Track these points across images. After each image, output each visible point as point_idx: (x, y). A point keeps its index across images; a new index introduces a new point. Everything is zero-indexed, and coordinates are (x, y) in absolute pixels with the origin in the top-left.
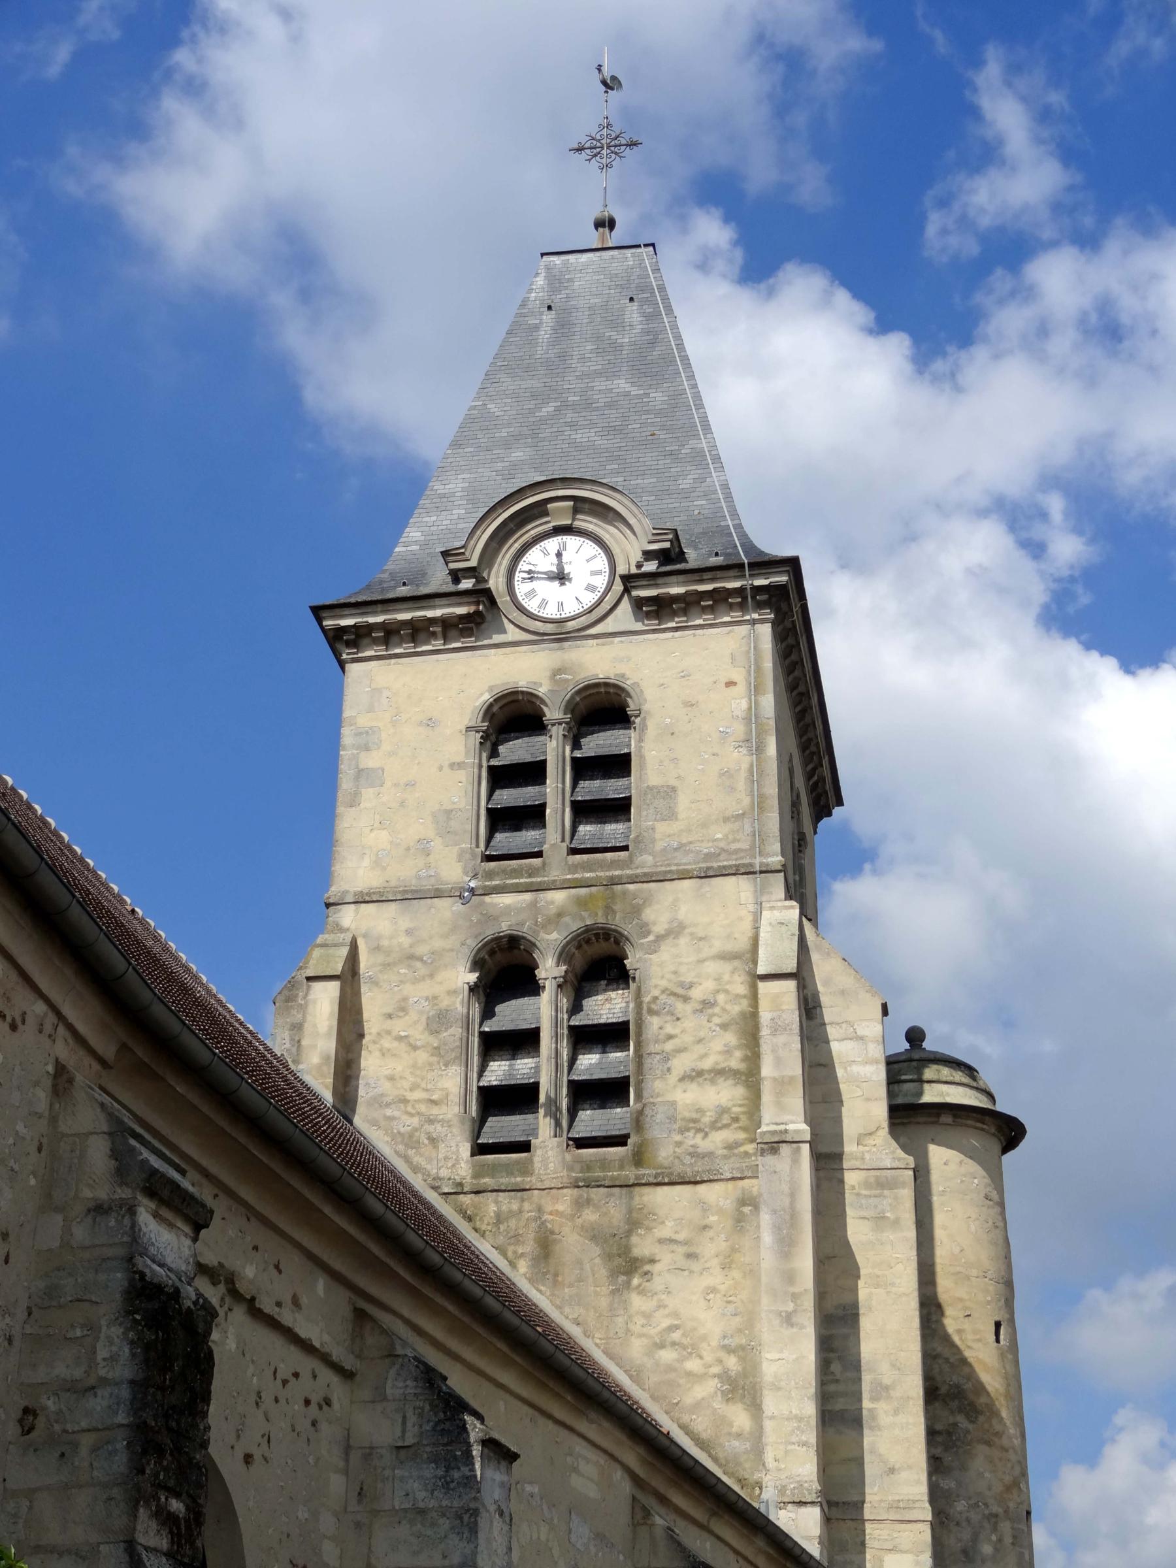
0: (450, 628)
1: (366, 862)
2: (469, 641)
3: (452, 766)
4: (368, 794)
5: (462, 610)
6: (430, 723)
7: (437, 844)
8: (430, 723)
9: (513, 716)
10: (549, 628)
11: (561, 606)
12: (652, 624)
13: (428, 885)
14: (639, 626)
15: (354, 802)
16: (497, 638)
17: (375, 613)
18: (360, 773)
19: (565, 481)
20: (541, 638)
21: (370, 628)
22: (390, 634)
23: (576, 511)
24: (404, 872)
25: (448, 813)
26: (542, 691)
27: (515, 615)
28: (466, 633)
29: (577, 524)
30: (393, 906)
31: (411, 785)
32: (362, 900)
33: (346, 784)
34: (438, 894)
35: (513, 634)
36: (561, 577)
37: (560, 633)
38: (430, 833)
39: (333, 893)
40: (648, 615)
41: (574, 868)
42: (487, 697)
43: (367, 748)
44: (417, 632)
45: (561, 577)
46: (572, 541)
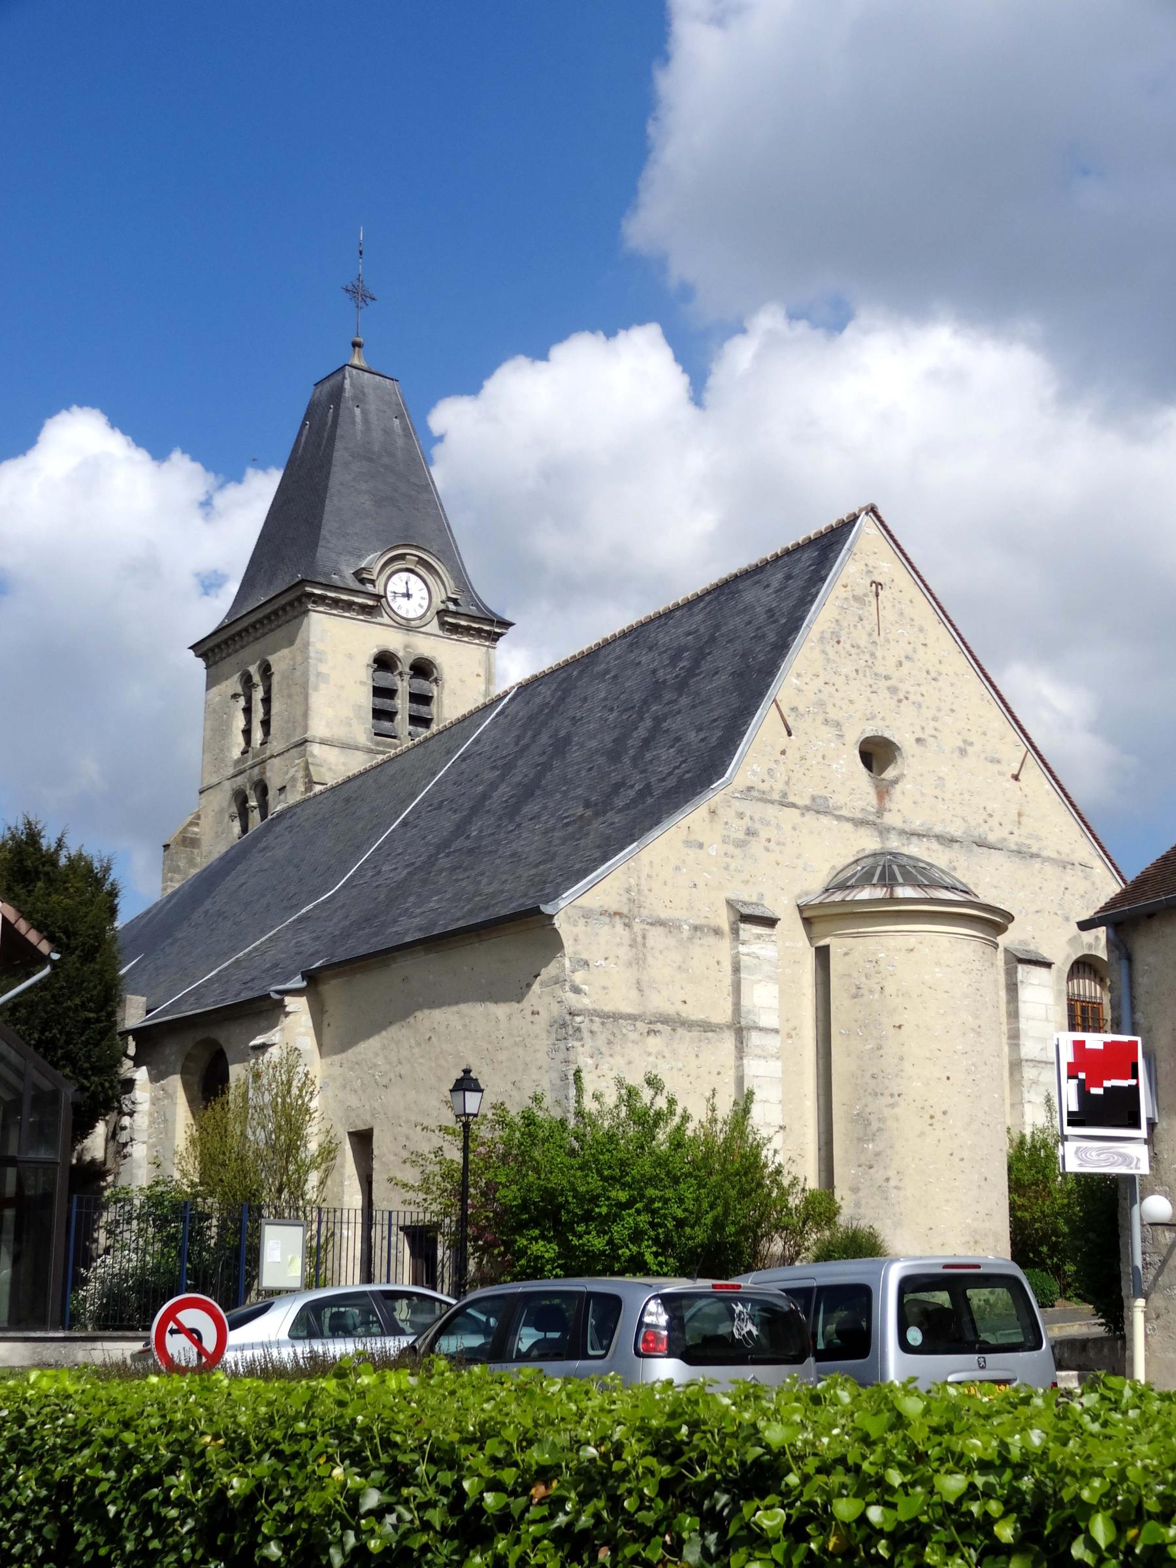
0: (365, 610)
1: (323, 723)
2: (368, 618)
3: (361, 682)
4: (322, 686)
5: (371, 603)
6: (350, 656)
7: (354, 722)
8: (350, 656)
9: (384, 661)
10: (403, 622)
11: (407, 612)
12: (447, 634)
13: (352, 742)
14: (440, 633)
15: (316, 689)
16: (379, 620)
17: (330, 591)
18: (318, 674)
19: (417, 547)
20: (400, 626)
21: (326, 597)
22: (336, 603)
23: (418, 563)
24: (339, 733)
25: (360, 707)
26: (400, 654)
27: (388, 610)
28: (369, 614)
29: (417, 570)
30: (337, 749)
31: (342, 687)
32: (323, 742)
33: (312, 679)
34: (357, 748)
35: (386, 619)
36: (408, 596)
37: (406, 626)
38: (352, 716)
39: (308, 735)
40: (448, 630)
41: (378, 744)
42: (375, 651)
43: (321, 661)
44: (349, 606)
45: (408, 596)
46: (413, 577)
